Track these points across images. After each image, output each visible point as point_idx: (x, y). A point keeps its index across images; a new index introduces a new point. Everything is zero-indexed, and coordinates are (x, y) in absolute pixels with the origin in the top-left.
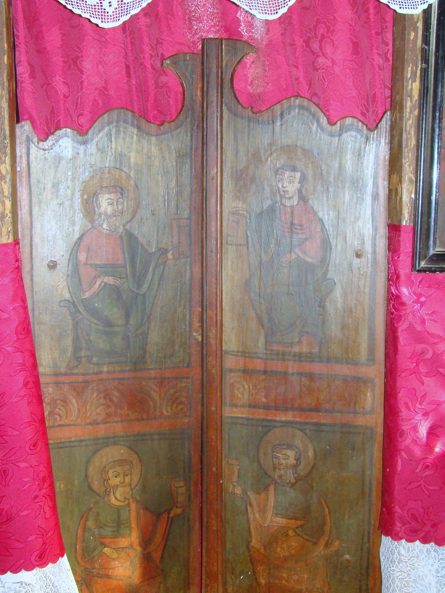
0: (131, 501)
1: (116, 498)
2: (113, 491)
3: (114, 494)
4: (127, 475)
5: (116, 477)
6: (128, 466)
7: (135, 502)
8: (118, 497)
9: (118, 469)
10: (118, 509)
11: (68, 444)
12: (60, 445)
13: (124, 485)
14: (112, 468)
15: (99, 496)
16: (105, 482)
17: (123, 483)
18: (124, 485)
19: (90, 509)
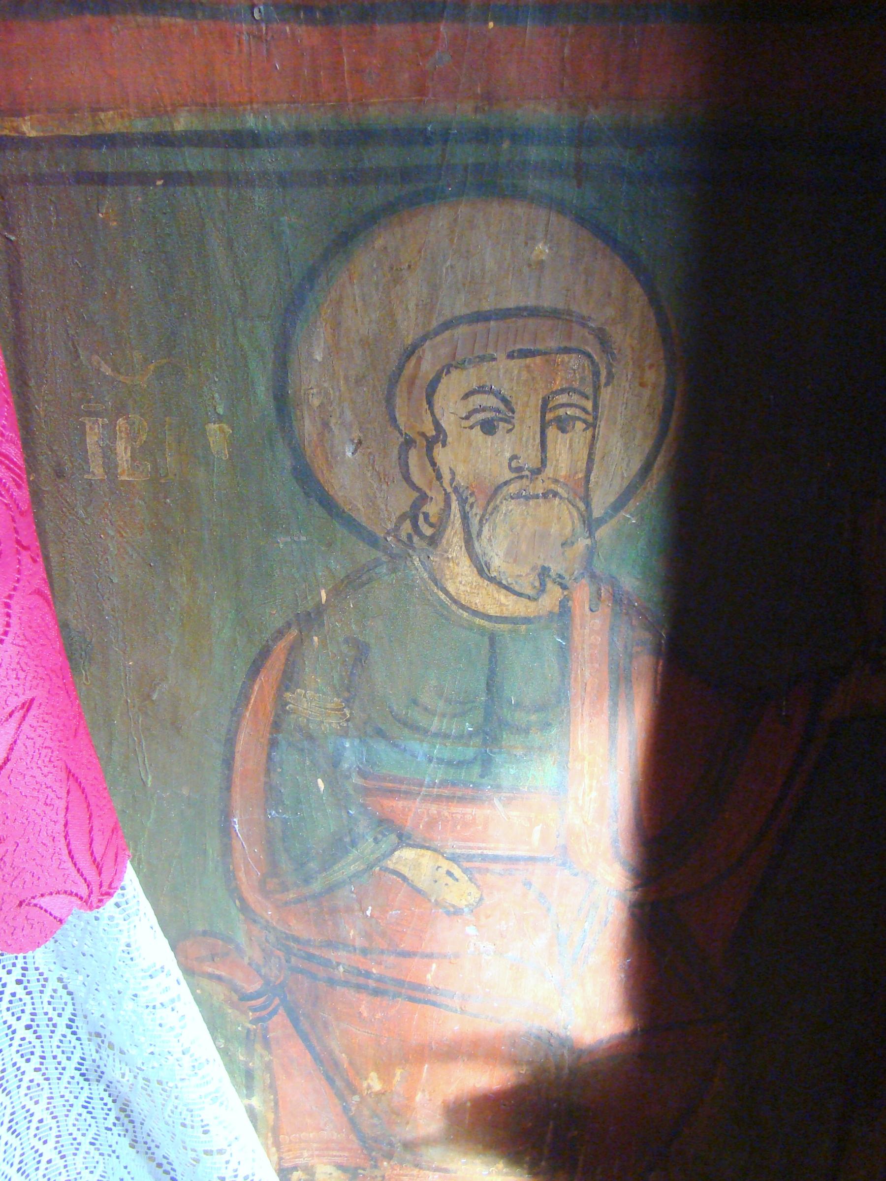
0: (582, 593)
1: (482, 569)
2: (465, 517)
3: (469, 542)
4: (563, 425)
5: (488, 428)
6: (573, 361)
7: (606, 608)
8: (498, 562)
9: (506, 374)
10: (493, 639)
11: (150, 159)
12: (99, 160)
13: (539, 487)
14: (460, 366)
15: (373, 541)
16: (414, 458)
17: (536, 472)
18: (539, 487)
19: (311, 619)
